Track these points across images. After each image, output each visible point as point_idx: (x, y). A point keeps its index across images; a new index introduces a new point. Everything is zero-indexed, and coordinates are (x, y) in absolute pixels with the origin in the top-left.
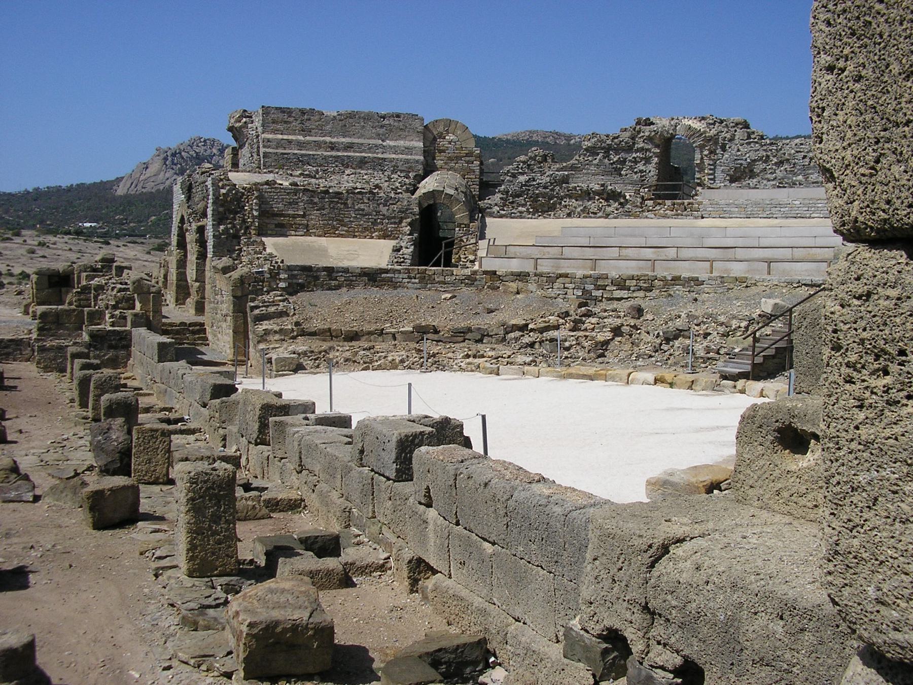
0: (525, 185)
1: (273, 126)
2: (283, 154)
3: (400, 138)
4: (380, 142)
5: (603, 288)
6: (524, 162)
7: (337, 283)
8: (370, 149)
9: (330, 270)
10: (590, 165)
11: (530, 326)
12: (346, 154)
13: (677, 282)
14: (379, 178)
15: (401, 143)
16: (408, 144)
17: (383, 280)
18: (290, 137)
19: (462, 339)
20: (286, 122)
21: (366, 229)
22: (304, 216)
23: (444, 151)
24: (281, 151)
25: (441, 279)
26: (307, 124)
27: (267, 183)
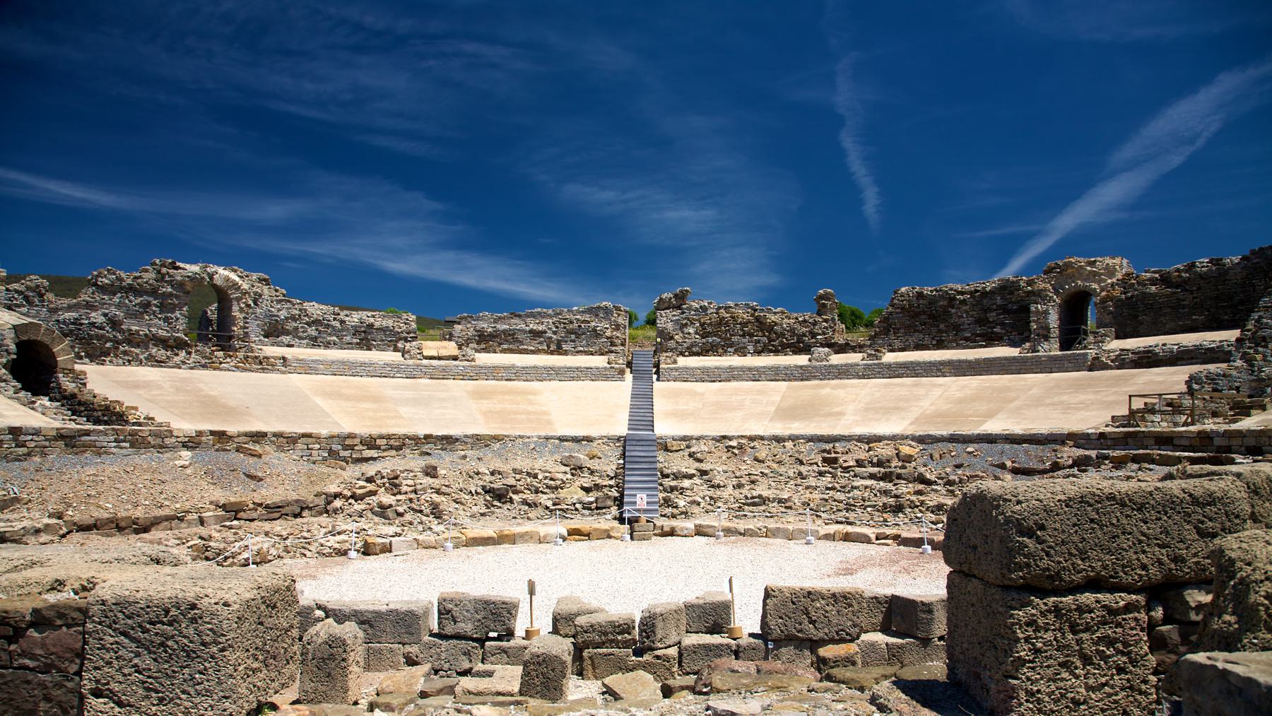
5: (352, 447)
7: (24, 450)
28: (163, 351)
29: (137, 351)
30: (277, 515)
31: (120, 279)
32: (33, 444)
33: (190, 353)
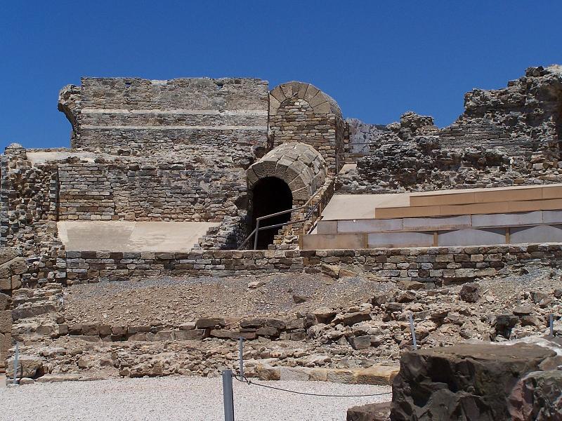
0: (386, 154)
1: (93, 100)
2: (103, 130)
3: (241, 106)
4: (217, 112)
5: (443, 266)
6: (395, 130)
7: (126, 271)
8: (204, 120)
9: (117, 257)
10: (474, 127)
11: (338, 317)
12: (176, 127)
13: (535, 254)
14: (211, 154)
15: (242, 112)
16: (250, 113)
18: (113, 111)
19: (253, 335)
20: (109, 95)
21: (184, 211)
22: (111, 196)
24: (102, 126)
25: (251, 263)
27: (69, 160)
29: (446, 173)
30: (253, 335)
31: (485, 99)
32: (133, 267)
33: (503, 170)
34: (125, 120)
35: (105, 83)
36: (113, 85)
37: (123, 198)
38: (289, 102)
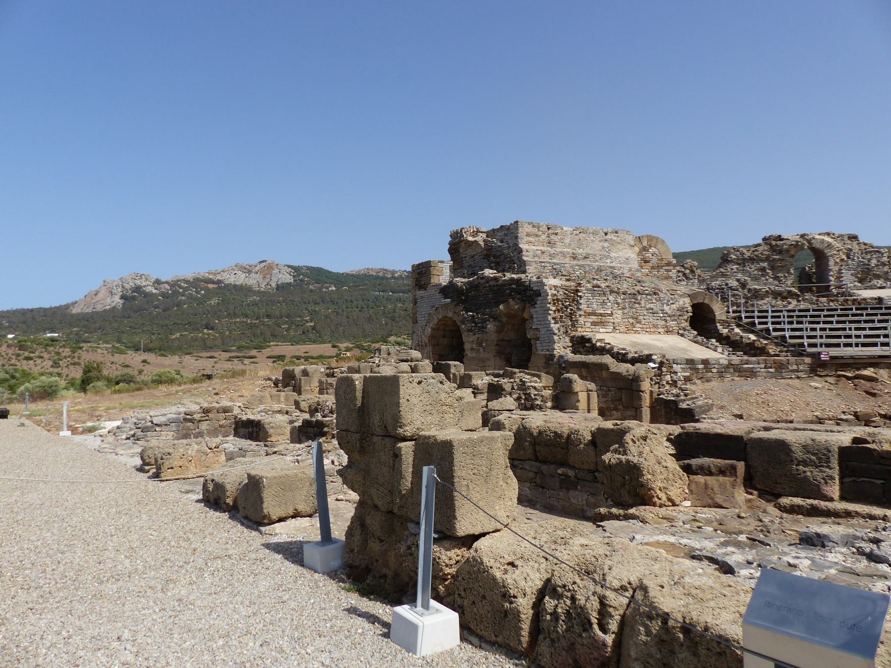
16: (627, 256)
17: (746, 370)
18: (542, 248)
20: (537, 236)
22: (611, 314)
23: (648, 262)
24: (536, 259)
25: (795, 367)
26: (552, 237)
28: (780, 302)
34: (552, 256)
35: (534, 226)
36: (539, 228)
37: (618, 315)
38: (645, 249)
